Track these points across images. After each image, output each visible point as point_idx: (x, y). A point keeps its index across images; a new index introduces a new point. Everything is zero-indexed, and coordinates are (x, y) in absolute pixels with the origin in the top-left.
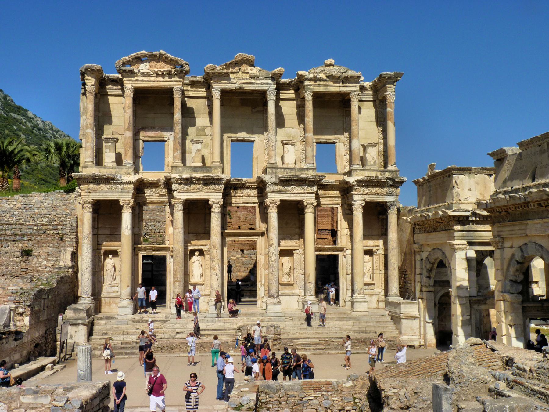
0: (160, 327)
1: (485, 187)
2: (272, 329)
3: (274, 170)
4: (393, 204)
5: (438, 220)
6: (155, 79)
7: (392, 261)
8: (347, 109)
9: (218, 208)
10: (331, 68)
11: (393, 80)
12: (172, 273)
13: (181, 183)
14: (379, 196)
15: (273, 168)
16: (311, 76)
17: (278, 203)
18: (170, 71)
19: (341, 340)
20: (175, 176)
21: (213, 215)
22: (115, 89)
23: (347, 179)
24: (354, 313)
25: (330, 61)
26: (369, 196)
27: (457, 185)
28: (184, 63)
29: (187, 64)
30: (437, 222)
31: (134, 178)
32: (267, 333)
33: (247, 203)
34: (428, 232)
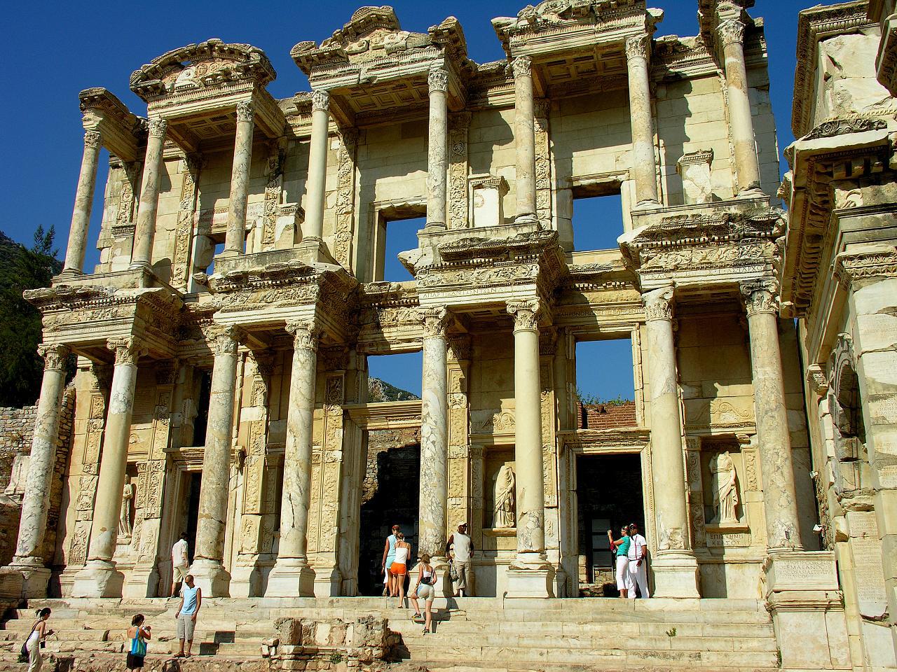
3: (435, 238)
4: (757, 287)
6: (206, 94)
9: (305, 340)
13: (228, 292)
14: (713, 272)
15: (431, 235)
17: (442, 315)
21: (295, 356)
26: (684, 274)
28: (250, 50)
29: (254, 51)
31: (141, 290)
33: (409, 341)
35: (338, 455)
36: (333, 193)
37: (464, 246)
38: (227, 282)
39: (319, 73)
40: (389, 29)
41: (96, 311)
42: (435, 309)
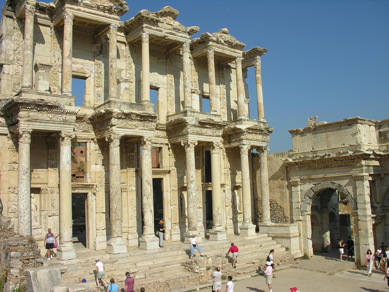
0: (112, 269)
1: (370, 135)
2: (219, 258)
3: (192, 113)
5: (336, 159)
7: (266, 194)
8: (222, 72)
10: (226, 35)
11: (260, 53)
12: (94, 212)
13: (120, 118)
14: (258, 142)
16: (215, 39)
17: (197, 144)
18: (111, 8)
19: (259, 261)
20: (116, 110)
22: (42, 18)
23: (238, 126)
24: (248, 238)
25: (225, 30)
26: (252, 141)
27: (359, 131)
28: (125, 2)
29: (126, 4)
30: (335, 160)
32: (213, 263)
33: (156, 144)
34: (315, 169)
35: (134, 188)
36: (123, 70)
37: (207, 121)
38: (122, 115)
39: (147, 25)
40: (173, 18)
41: (53, 115)
42: (194, 142)
